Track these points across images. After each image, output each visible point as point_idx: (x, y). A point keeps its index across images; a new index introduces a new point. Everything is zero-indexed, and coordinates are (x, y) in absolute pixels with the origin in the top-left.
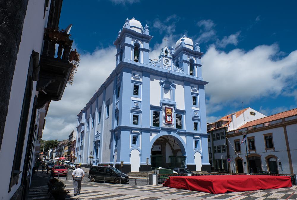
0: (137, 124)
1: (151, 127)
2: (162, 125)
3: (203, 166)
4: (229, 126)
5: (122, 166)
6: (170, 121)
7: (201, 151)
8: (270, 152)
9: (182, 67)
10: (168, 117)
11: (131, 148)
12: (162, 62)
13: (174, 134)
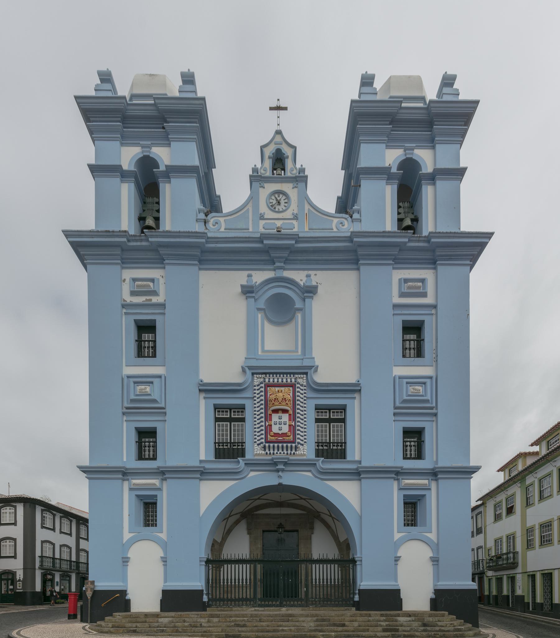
1: (201, 461)
6: (284, 435)
12: (256, 207)
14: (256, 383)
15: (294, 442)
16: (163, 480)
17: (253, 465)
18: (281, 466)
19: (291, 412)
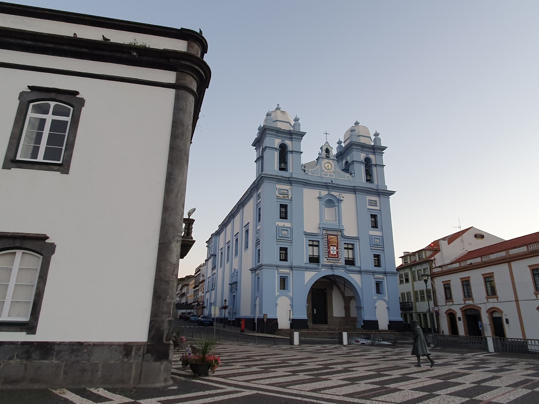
0: (286, 260)
1: (305, 263)
2: (324, 260)
3: (390, 322)
4: (435, 259)
5: (265, 320)
7: (386, 298)
8: (492, 303)
9: (353, 172)
10: (331, 248)
11: (277, 294)
12: (321, 167)
13: (340, 272)
14: (324, 233)
15: (338, 258)
16: (291, 270)
17: (323, 266)
18: (334, 268)
19: (337, 246)
